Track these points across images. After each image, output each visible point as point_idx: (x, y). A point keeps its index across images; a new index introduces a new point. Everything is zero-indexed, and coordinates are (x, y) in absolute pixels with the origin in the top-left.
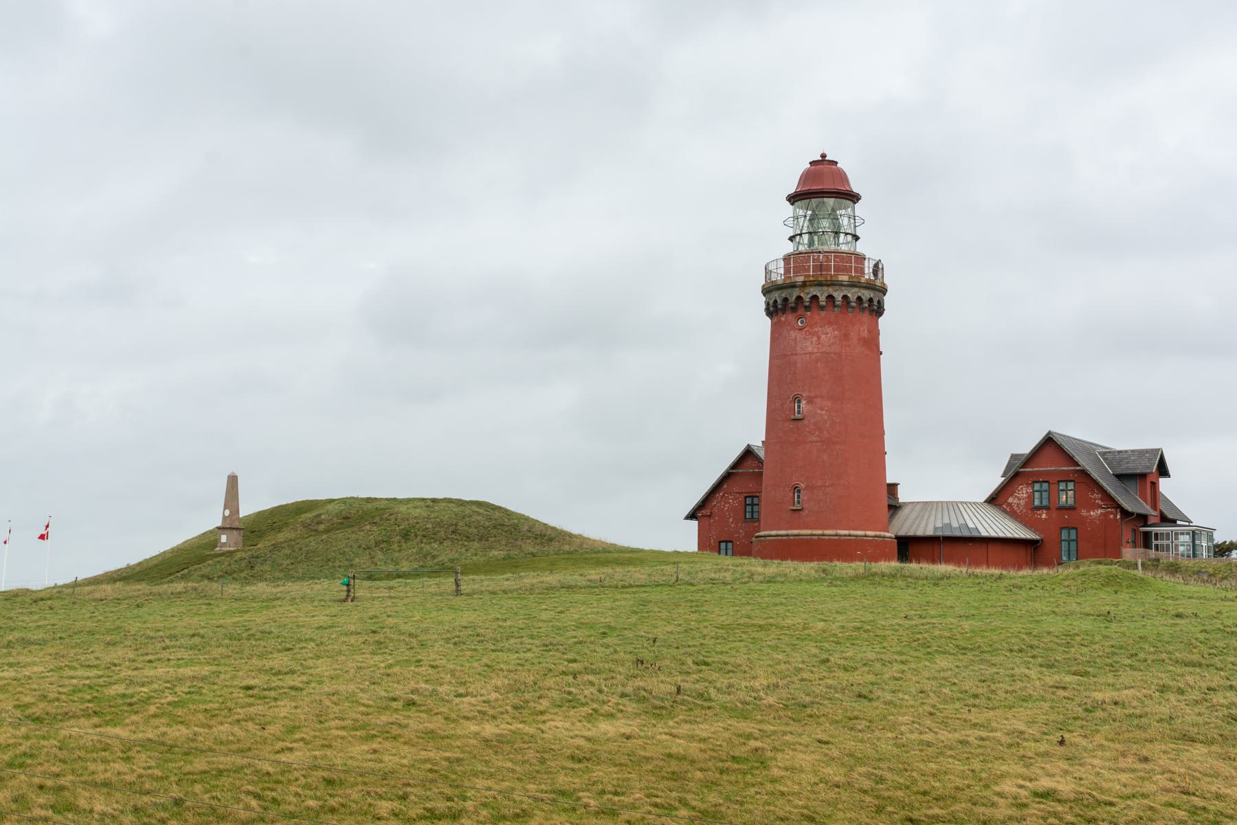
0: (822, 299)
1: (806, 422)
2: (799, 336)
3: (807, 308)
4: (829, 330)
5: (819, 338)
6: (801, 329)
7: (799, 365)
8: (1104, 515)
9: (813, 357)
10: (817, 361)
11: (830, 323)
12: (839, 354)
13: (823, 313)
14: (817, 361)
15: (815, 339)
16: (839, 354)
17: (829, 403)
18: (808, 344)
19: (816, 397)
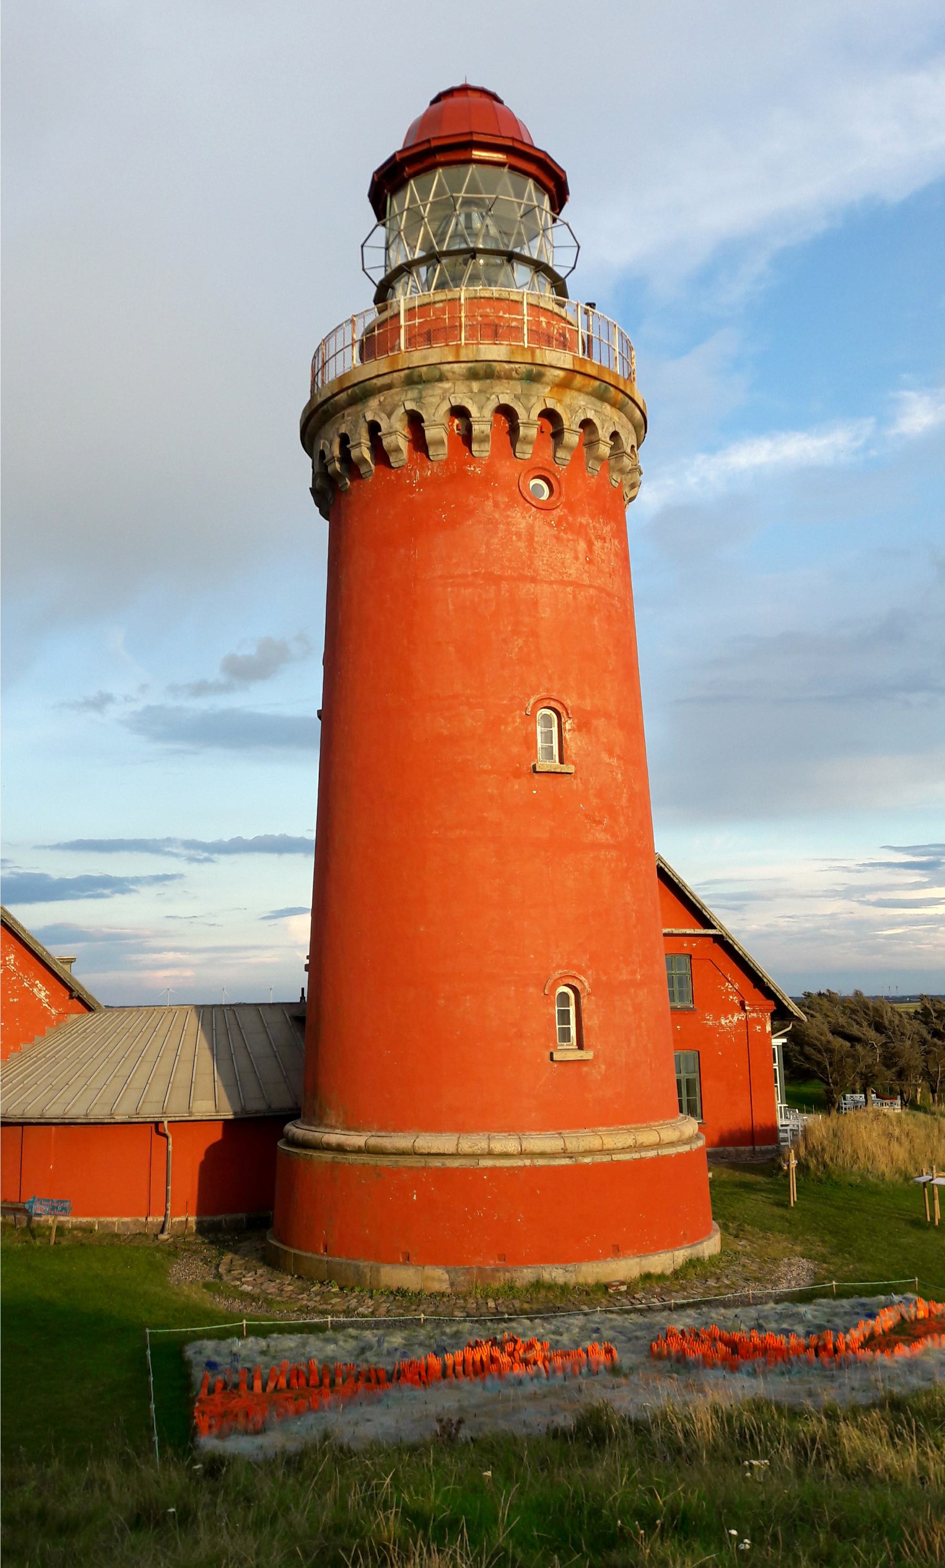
0: (604, 433)
1: (577, 784)
2: (543, 529)
5: (590, 545)
6: (545, 508)
7: (546, 613)
8: (747, 1023)
9: (581, 595)
15: (582, 546)
18: (569, 556)
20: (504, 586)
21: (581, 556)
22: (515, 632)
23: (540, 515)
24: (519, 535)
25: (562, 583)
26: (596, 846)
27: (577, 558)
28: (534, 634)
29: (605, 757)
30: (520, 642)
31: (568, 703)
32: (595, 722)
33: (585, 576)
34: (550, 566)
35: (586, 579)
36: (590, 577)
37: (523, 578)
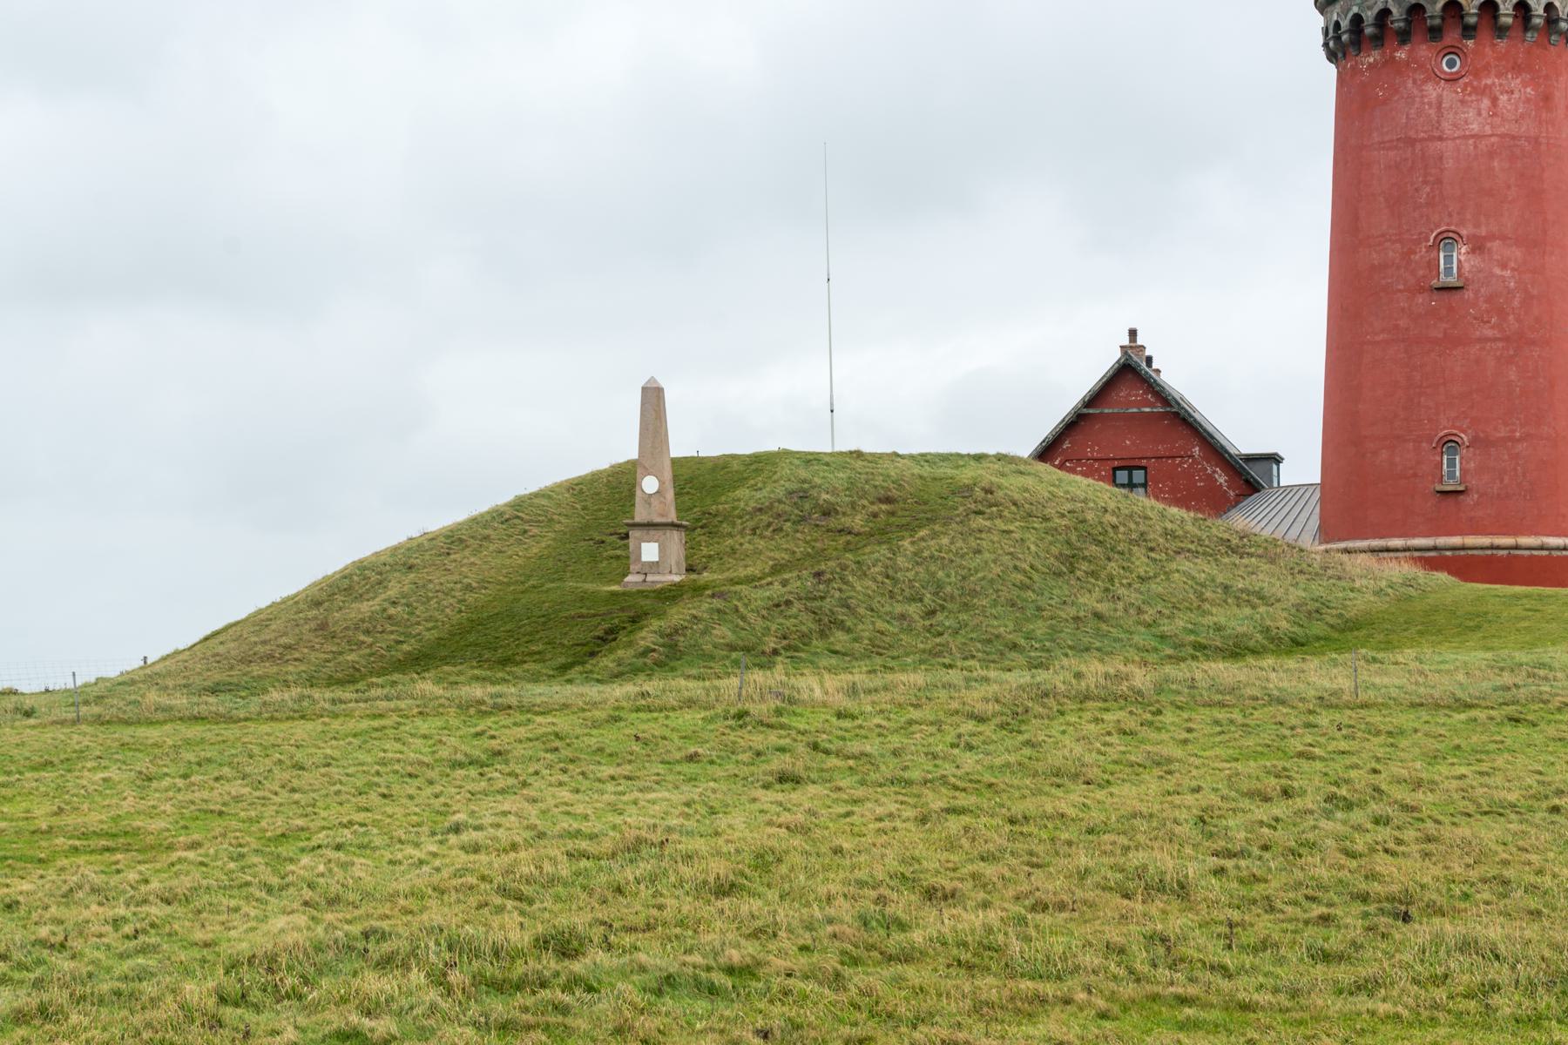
1: (1468, 294)
2: (1449, 95)
3: (1469, 31)
4: (1516, 83)
5: (1494, 100)
6: (1452, 80)
7: (1449, 164)
9: (1483, 145)
10: (1491, 154)
11: (1517, 69)
12: (1536, 141)
13: (1502, 44)
14: (1491, 154)
15: (1486, 103)
16: (1536, 141)
17: (1517, 253)
18: (1471, 114)
19: (1492, 237)
20: (1418, 146)
21: (1484, 113)
22: (1425, 182)
23: (1448, 86)
24: (1430, 104)
25: (1465, 137)
26: (1484, 340)
27: (1479, 114)
28: (1439, 182)
29: (1498, 271)
30: (1428, 189)
31: (1464, 232)
32: (1489, 245)
33: (1487, 128)
34: (1455, 125)
35: (1488, 129)
36: (1492, 127)
37: (1432, 139)
